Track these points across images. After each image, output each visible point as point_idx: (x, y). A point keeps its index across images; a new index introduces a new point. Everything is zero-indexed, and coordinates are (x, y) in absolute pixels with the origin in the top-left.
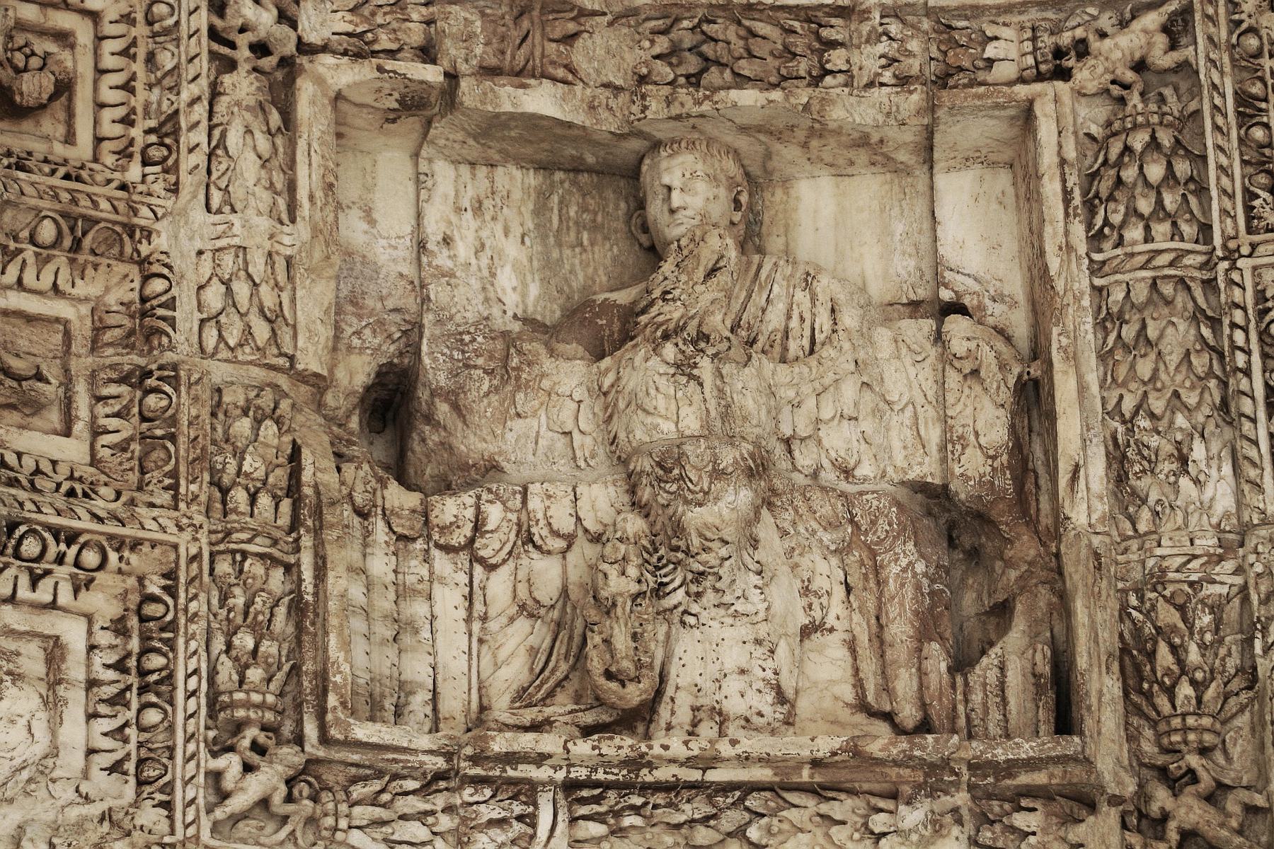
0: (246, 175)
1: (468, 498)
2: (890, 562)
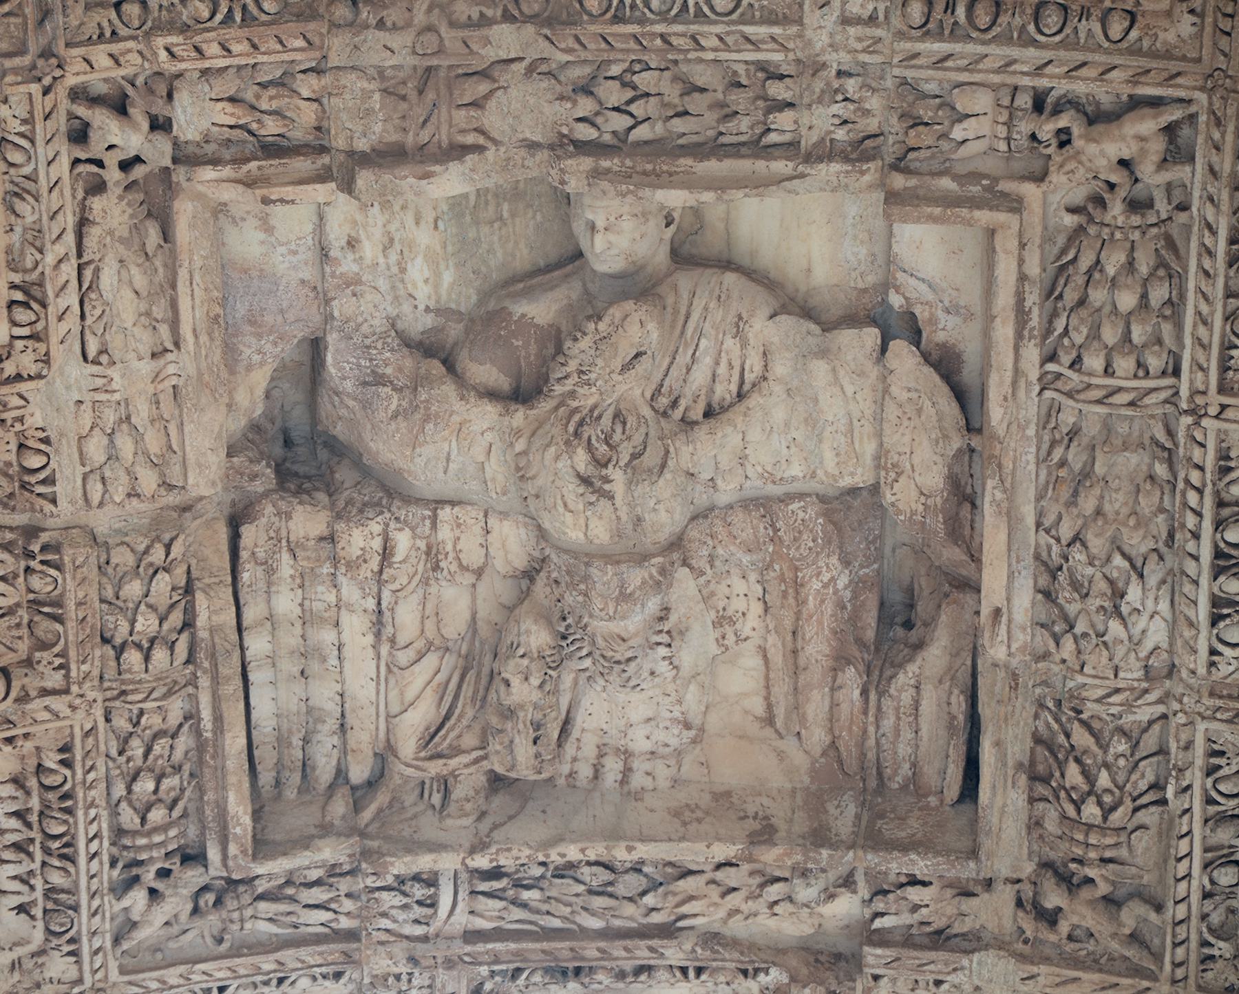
0: (124, 316)
1: (376, 527)
2: (811, 577)
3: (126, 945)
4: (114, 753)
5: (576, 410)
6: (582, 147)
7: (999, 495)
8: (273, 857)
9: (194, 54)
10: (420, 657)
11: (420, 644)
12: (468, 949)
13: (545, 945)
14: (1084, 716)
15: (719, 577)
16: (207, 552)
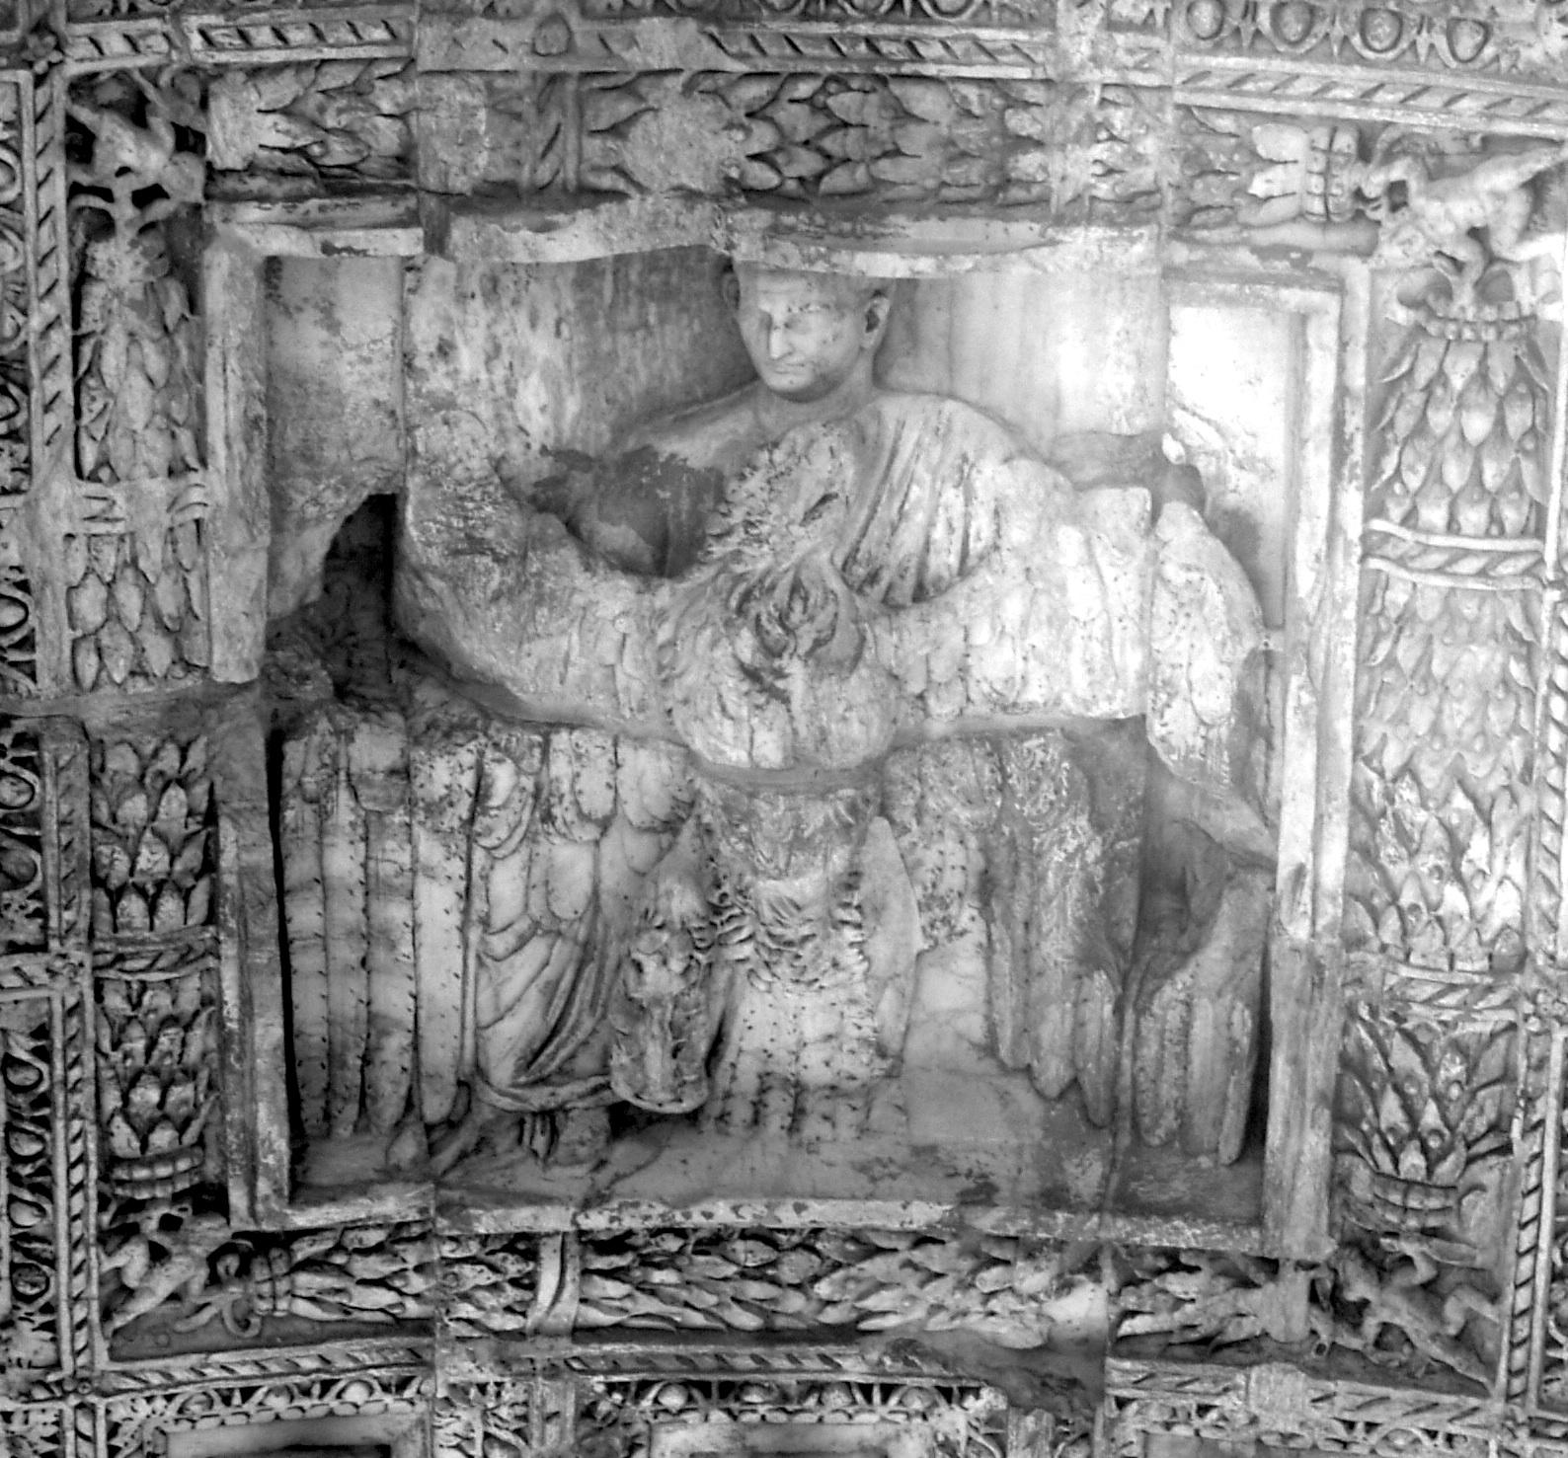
3: (119, 1322)
4: (106, 1045)
5: (741, 577)
6: (756, 196)
7: (1307, 699)
8: (318, 1203)
9: (238, 42)
10: (523, 942)
11: (523, 926)
12: (578, 1350)
13: (681, 1349)
14: (1408, 1026)
15: (929, 838)
16: (237, 767)
